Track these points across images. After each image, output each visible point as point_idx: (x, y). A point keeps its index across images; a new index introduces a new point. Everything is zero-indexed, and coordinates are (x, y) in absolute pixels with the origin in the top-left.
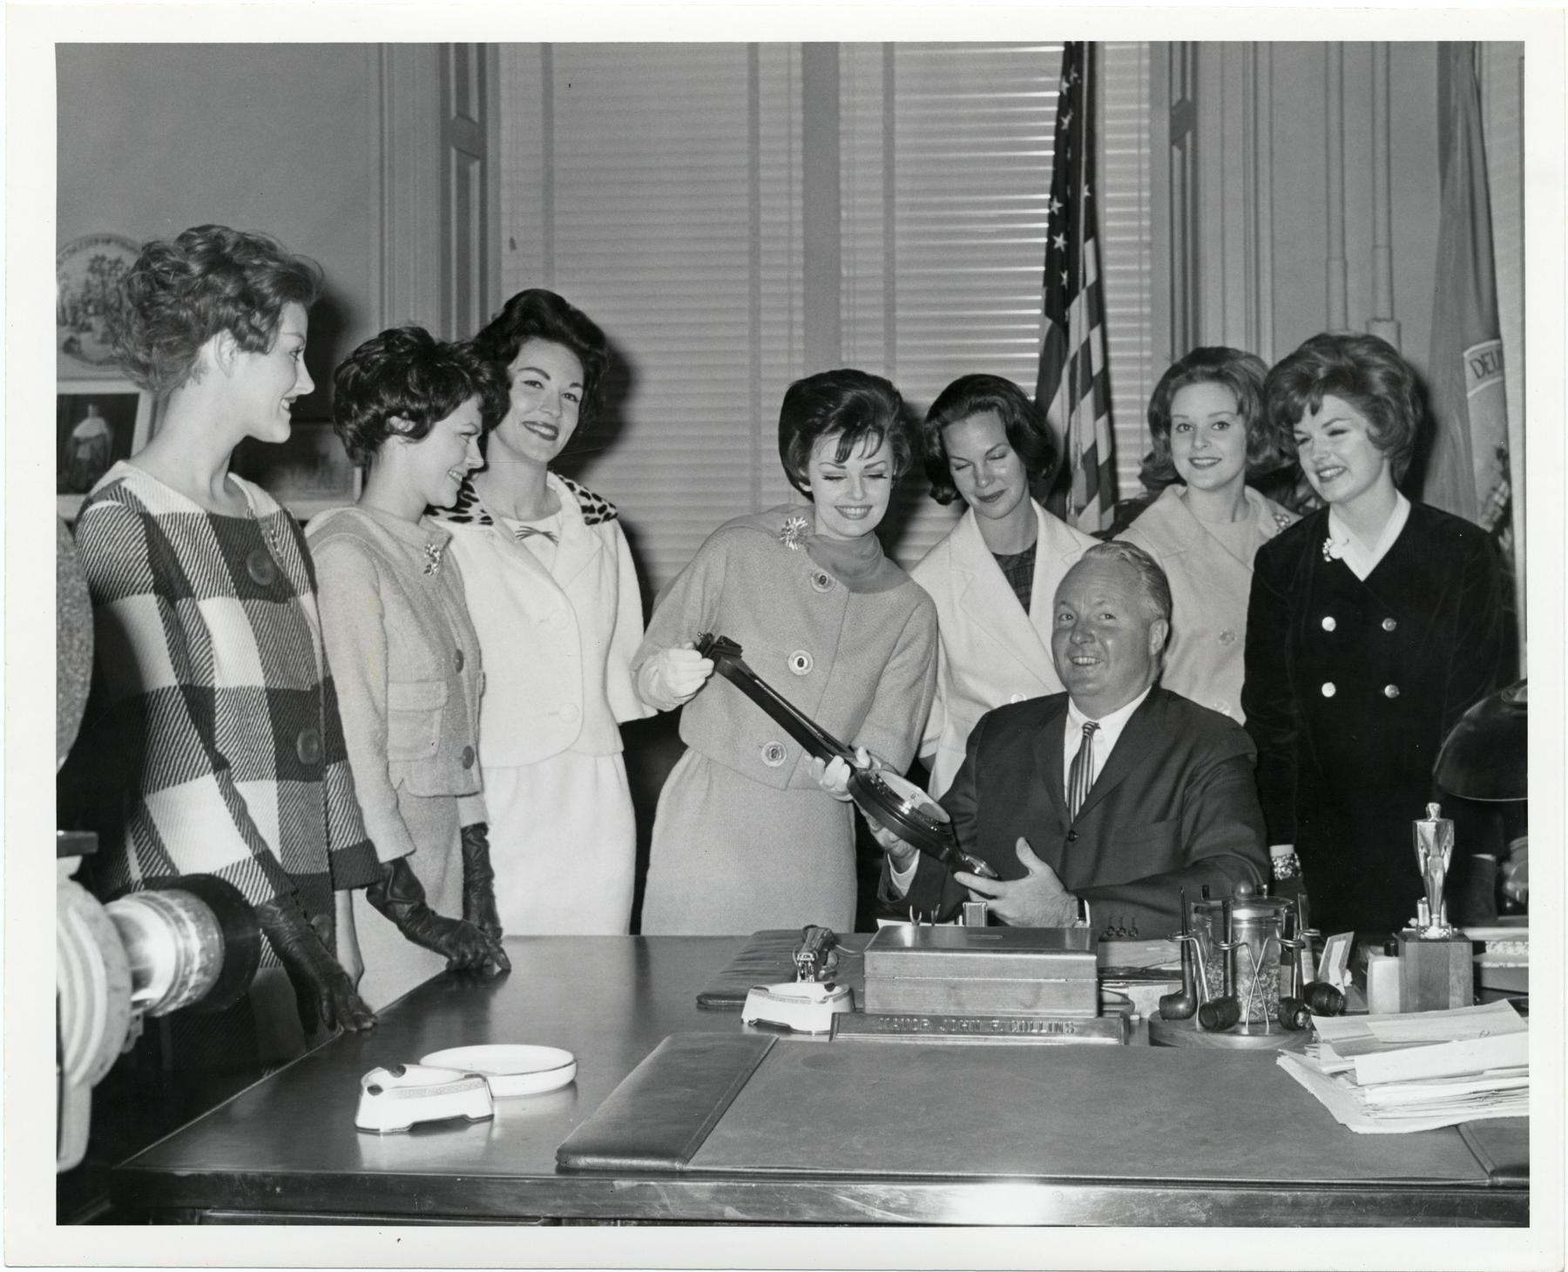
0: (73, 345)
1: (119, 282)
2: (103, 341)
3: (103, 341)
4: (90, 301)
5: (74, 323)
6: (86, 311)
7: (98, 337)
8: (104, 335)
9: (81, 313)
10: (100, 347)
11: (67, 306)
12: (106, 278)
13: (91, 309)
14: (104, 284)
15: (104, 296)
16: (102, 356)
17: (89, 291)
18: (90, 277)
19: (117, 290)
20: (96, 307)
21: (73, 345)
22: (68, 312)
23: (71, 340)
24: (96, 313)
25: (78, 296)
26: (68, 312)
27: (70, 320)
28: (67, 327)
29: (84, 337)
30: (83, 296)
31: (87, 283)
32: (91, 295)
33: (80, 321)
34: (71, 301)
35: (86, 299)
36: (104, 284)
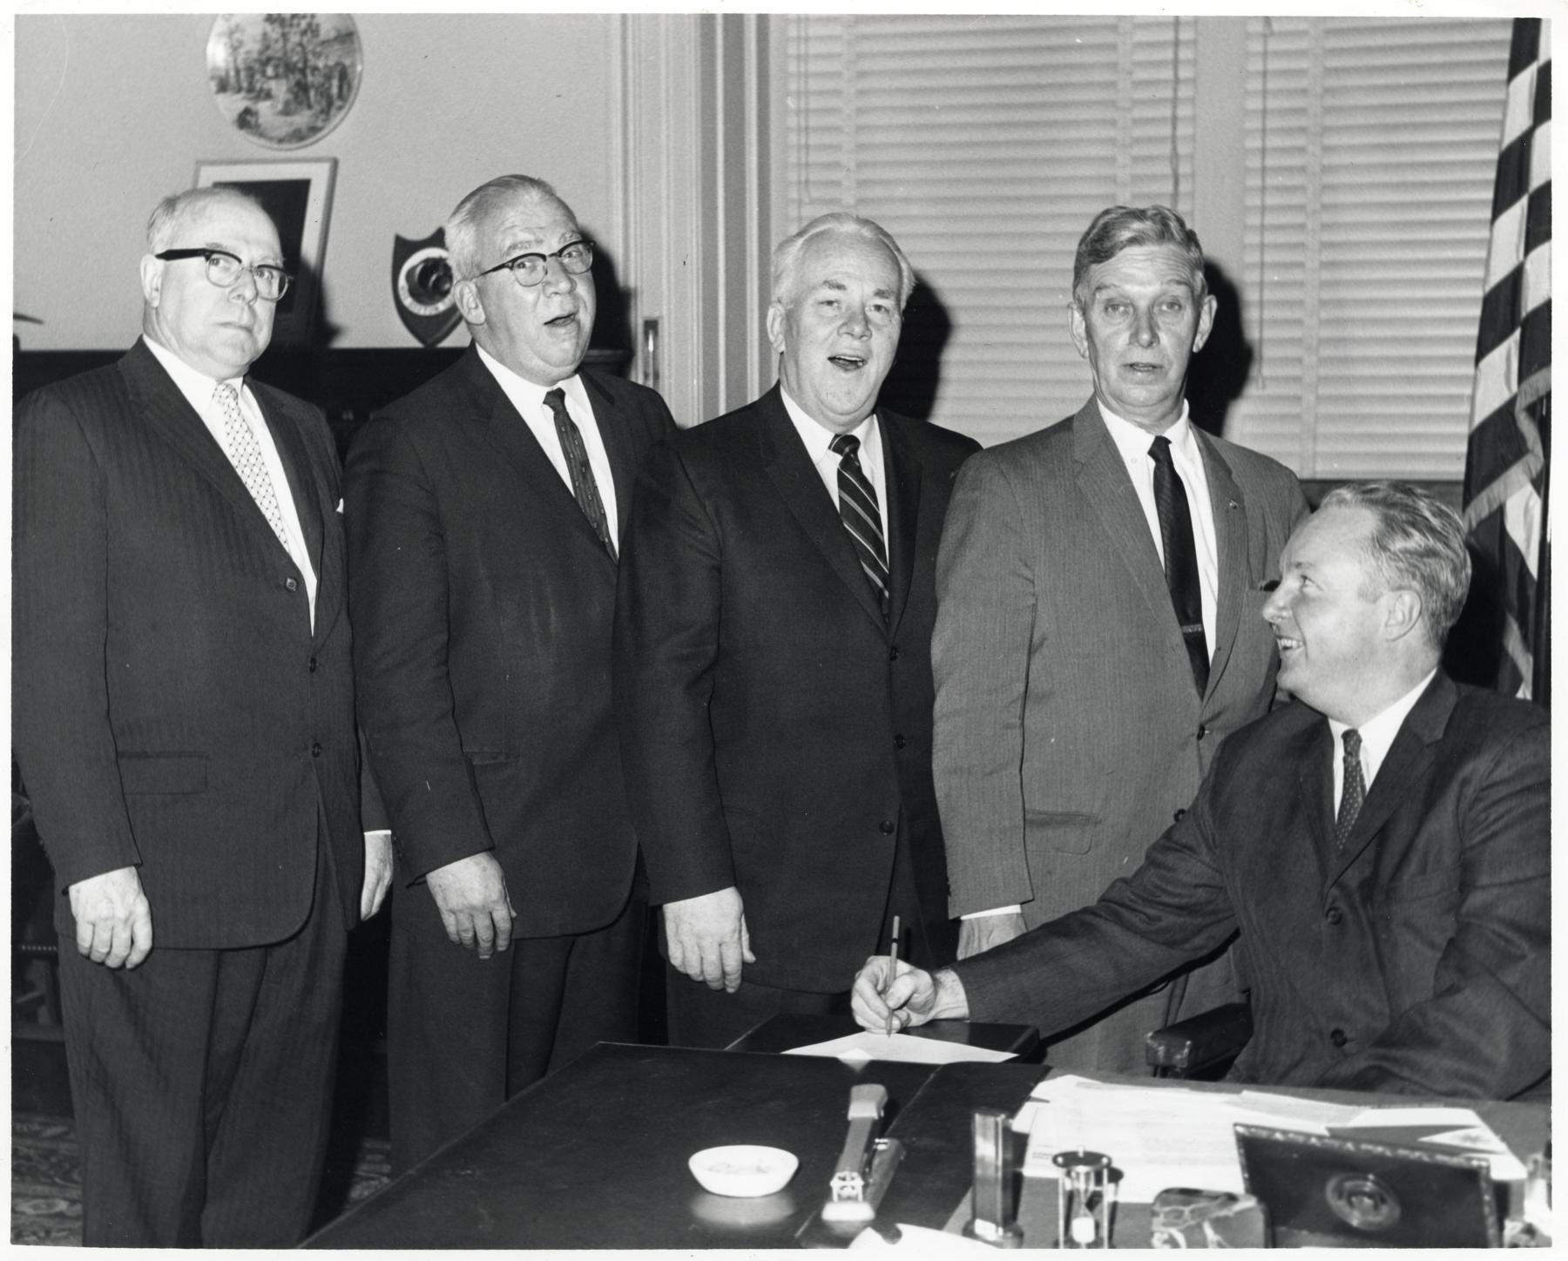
0: (249, 118)
1: (304, 33)
2: (286, 112)
3: (286, 112)
4: (269, 60)
5: (250, 90)
6: (264, 73)
7: (280, 107)
8: (287, 103)
9: (258, 77)
10: (282, 119)
11: (241, 66)
12: (287, 30)
13: (270, 71)
14: (284, 36)
15: (285, 53)
16: (284, 131)
17: (268, 47)
18: (269, 28)
19: (300, 44)
20: (276, 67)
21: (249, 118)
22: (243, 74)
23: (247, 111)
24: (276, 76)
25: (255, 55)
26: (243, 74)
27: (245, 85)
28: (242, 95)
29: (263, 107)
30: (261, 53)
31: (265, 35)
32: (269, 53)
33: (258, 86)
34: (245, 60)
35: (264, 57)
36: (284, 36)
